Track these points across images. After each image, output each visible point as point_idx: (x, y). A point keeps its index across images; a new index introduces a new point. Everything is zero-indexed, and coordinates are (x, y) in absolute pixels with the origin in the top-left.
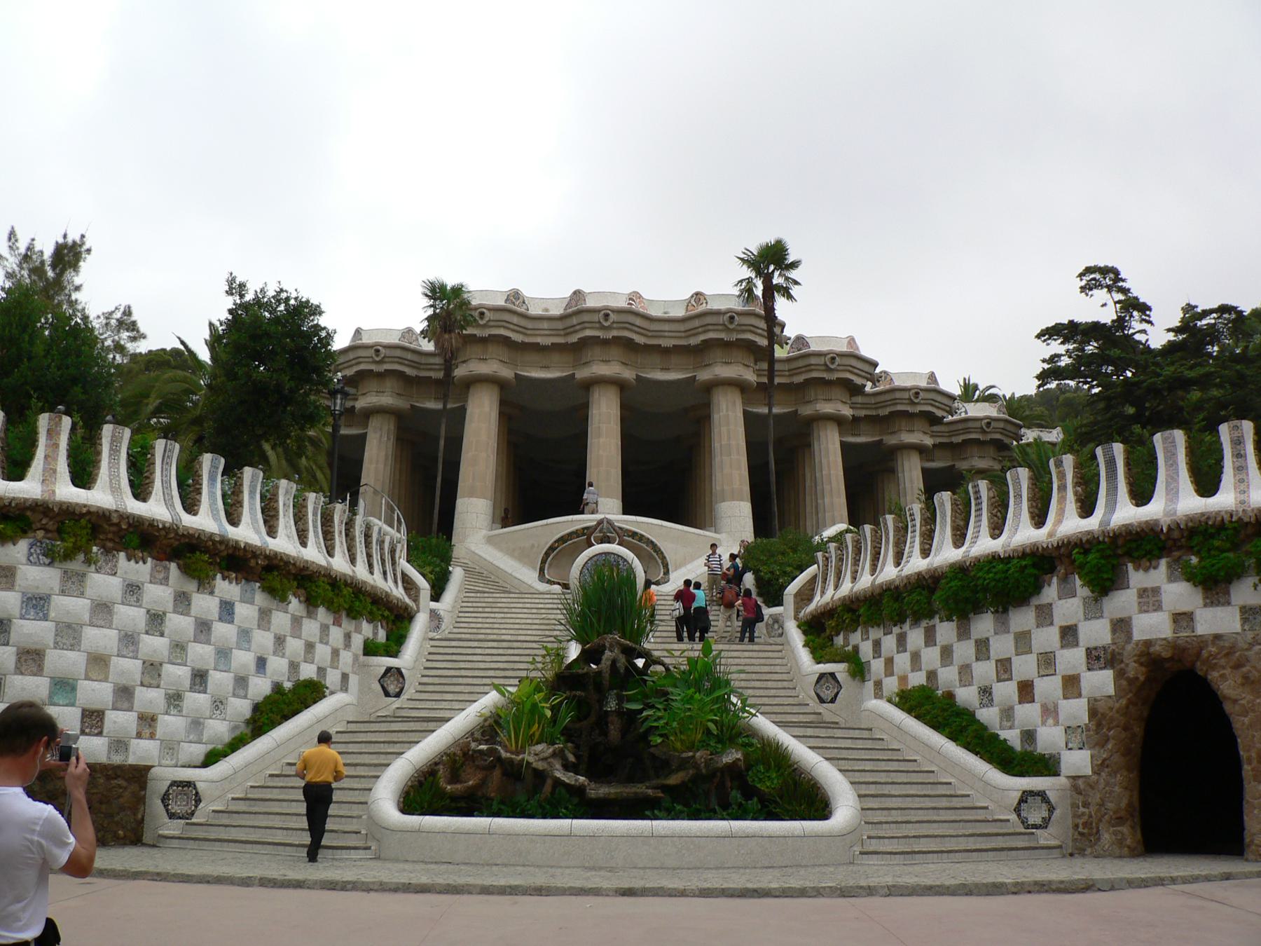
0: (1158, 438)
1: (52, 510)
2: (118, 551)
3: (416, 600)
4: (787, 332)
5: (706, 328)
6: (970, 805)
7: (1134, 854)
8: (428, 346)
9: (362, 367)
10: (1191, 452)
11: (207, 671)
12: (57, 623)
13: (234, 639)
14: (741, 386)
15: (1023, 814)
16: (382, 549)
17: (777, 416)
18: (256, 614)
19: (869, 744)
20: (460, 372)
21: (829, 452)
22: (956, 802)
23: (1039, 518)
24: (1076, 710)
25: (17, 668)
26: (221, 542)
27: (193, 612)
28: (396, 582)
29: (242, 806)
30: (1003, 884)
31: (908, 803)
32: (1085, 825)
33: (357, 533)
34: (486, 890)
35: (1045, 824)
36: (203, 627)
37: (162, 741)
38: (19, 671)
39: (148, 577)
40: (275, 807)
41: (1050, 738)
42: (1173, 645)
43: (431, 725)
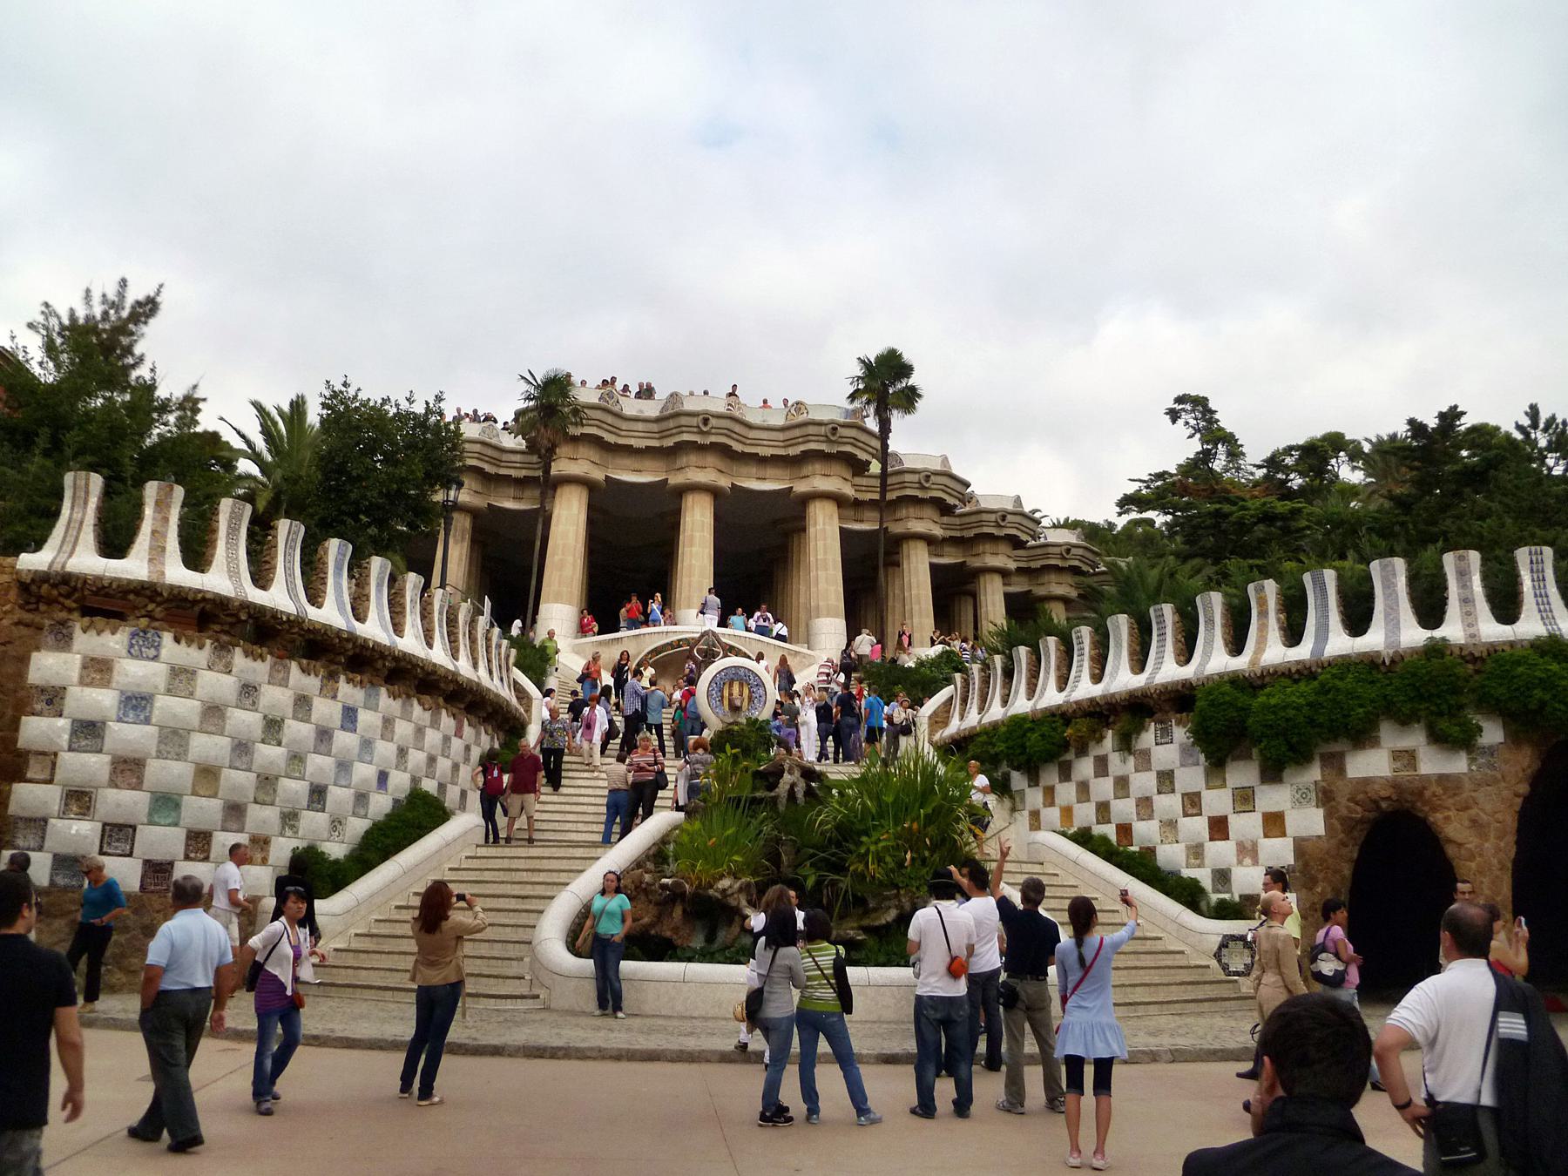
0: (1375, 566)
1: (161, 594)
2: (234, 646)
5: (806, 438)
8: (518, 443)
10: (1412, 580)
11: (326, 787)
13: (356, 751)
14: (839, 500)
21: (917, 569)
23: (1236, 645)
25: (111, 780)
26: (348, 640)
27: (313, 719)
36: (324, 735)
37: (275, 867)
38: (113, 784)
39: (266, 678)
42: (1395, 784)
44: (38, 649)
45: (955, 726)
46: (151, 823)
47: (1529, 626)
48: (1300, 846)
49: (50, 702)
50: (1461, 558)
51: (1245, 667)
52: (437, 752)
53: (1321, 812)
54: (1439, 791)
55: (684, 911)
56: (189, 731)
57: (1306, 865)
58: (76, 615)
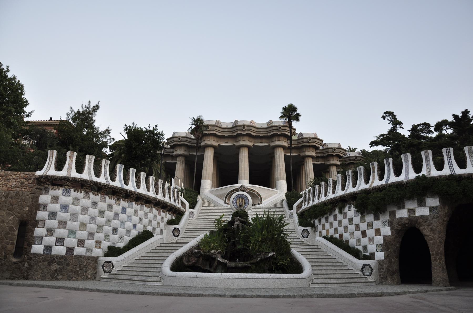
3: (185, 208)
4: (296, 132)
8: (193, 136)
9: (175, 143)
12: (71, 213)
13: (126, 219)
14: (283, 147)
15: (364, 272)
16: (174, 193)
17: (293, 156)
18: (133, 212)
19: (317, 250)
20: (202, 144)
22: (342, 268)
23: (367, 181)
24: (379, 240)
26: (122, 190)
27: (113, 211)
28: (179, 203)
29: (126, 269)
30: (354, 294)
31: (328, 268)
33: (166, 188)
34: (190, 295)
35: (370, 275)
36: (116, 215)
37: (103, 249)
40: (135, 269)
41: (372, 248)
42: (408, 219)
43: (183, 244)
44: (41, 194)
45: (304, 207)
46: (69, 238)
47: (446, 171)
48: (385, 238)
49: (44, 208)
50: (426, 152)
52: (152, 219)
53: (390, 228)
54: (421, 220)
55: (203, 259)
57: (386, 243)
58: (50, 186)
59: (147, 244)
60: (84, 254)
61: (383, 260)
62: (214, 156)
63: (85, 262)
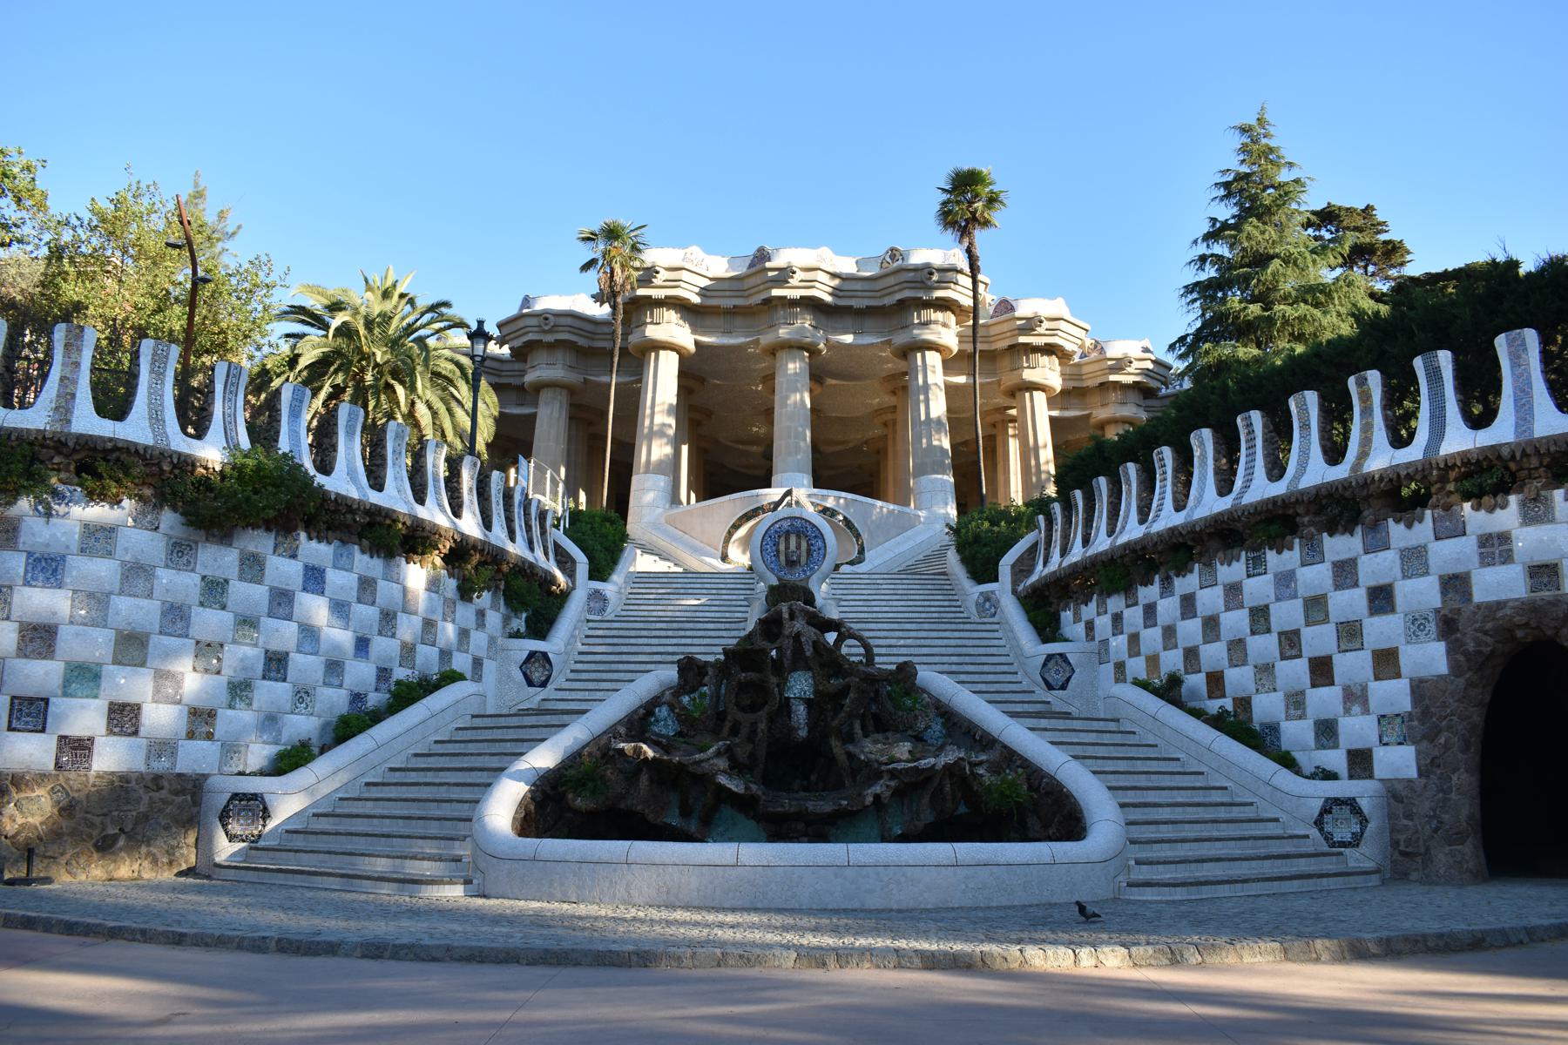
1: (66, 445)
6: (1252, 815)
7: (1479, 878)
15: (1328, 828)
18: (355, 584)
19: (1118, 739)
22: (1236, 813)
24: (1394, 694)
28: (546, 554)
31: (1178, 813)
32: (1408, 842)
35: (1356, 841)
43: (566, 717)
45: (1040, 572)
48: (1419, 688)
51: (1346, 475)
53: (1441, 647)
55: (651, 781)
56: (109, 594)
59: (416, 720)
60: (143, 768)
61: (1410, 781)
62: (680, 387)
63: (146, 799)
